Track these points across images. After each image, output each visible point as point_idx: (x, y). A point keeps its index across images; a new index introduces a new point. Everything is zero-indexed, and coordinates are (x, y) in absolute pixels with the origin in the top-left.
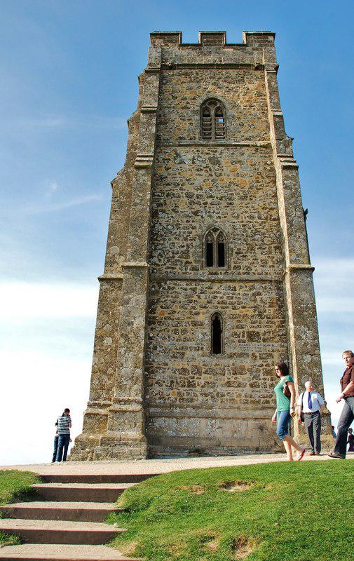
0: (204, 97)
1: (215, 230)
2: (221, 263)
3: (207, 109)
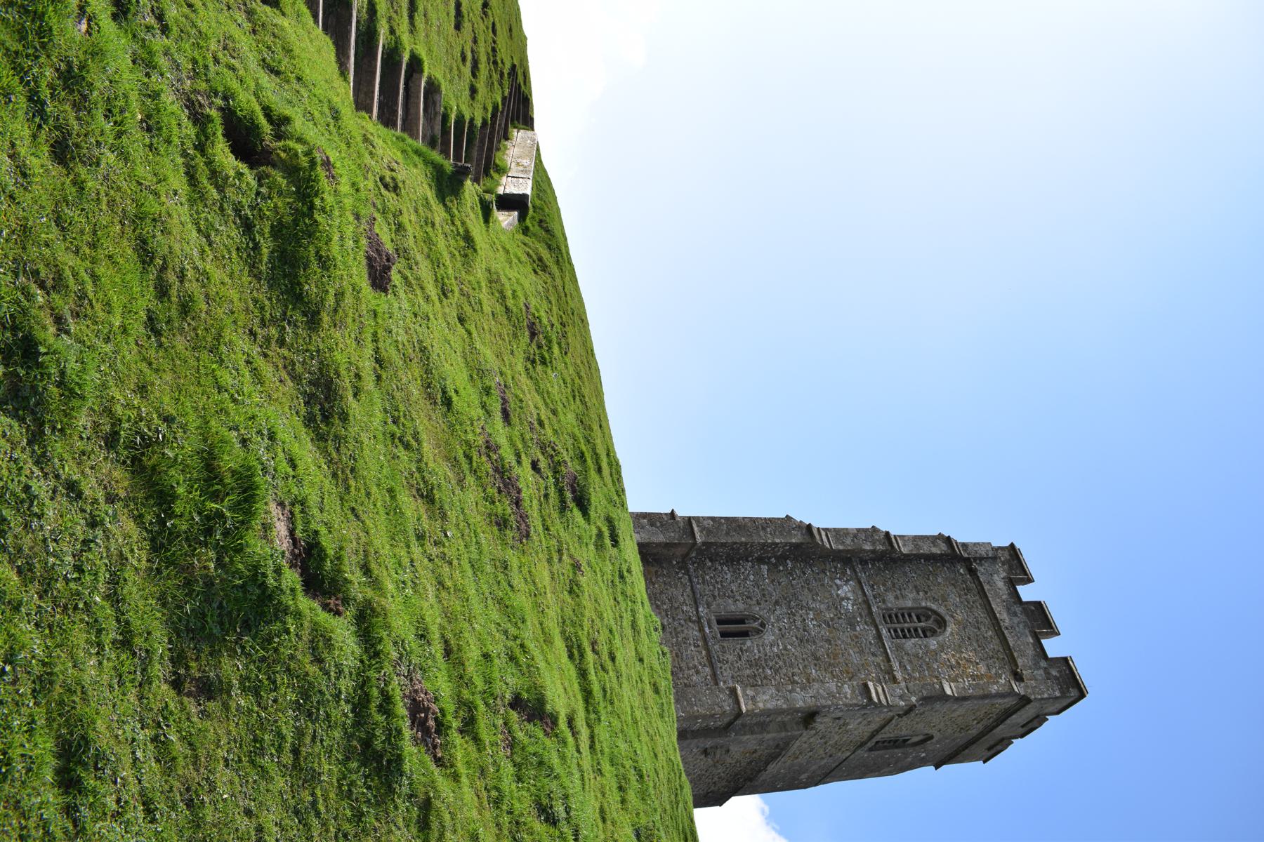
0: (942, 610)
1: (763, 625)
2: (724, 635)
3: (928, 618)
